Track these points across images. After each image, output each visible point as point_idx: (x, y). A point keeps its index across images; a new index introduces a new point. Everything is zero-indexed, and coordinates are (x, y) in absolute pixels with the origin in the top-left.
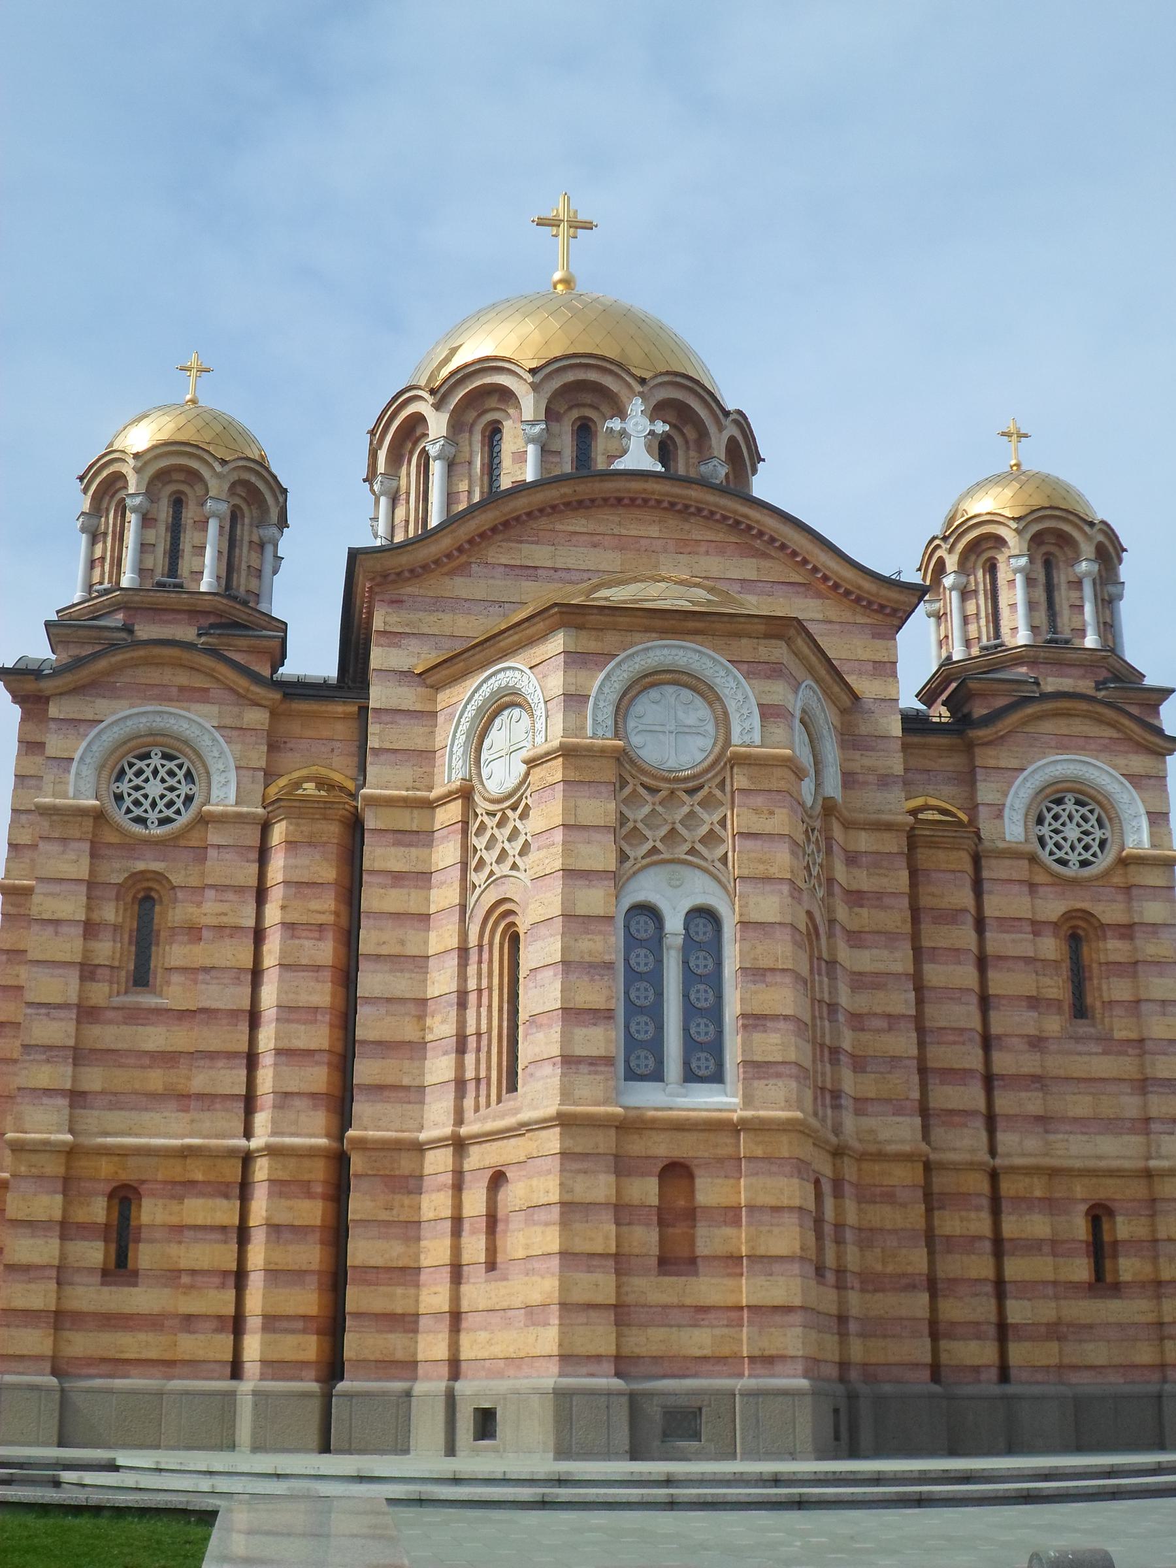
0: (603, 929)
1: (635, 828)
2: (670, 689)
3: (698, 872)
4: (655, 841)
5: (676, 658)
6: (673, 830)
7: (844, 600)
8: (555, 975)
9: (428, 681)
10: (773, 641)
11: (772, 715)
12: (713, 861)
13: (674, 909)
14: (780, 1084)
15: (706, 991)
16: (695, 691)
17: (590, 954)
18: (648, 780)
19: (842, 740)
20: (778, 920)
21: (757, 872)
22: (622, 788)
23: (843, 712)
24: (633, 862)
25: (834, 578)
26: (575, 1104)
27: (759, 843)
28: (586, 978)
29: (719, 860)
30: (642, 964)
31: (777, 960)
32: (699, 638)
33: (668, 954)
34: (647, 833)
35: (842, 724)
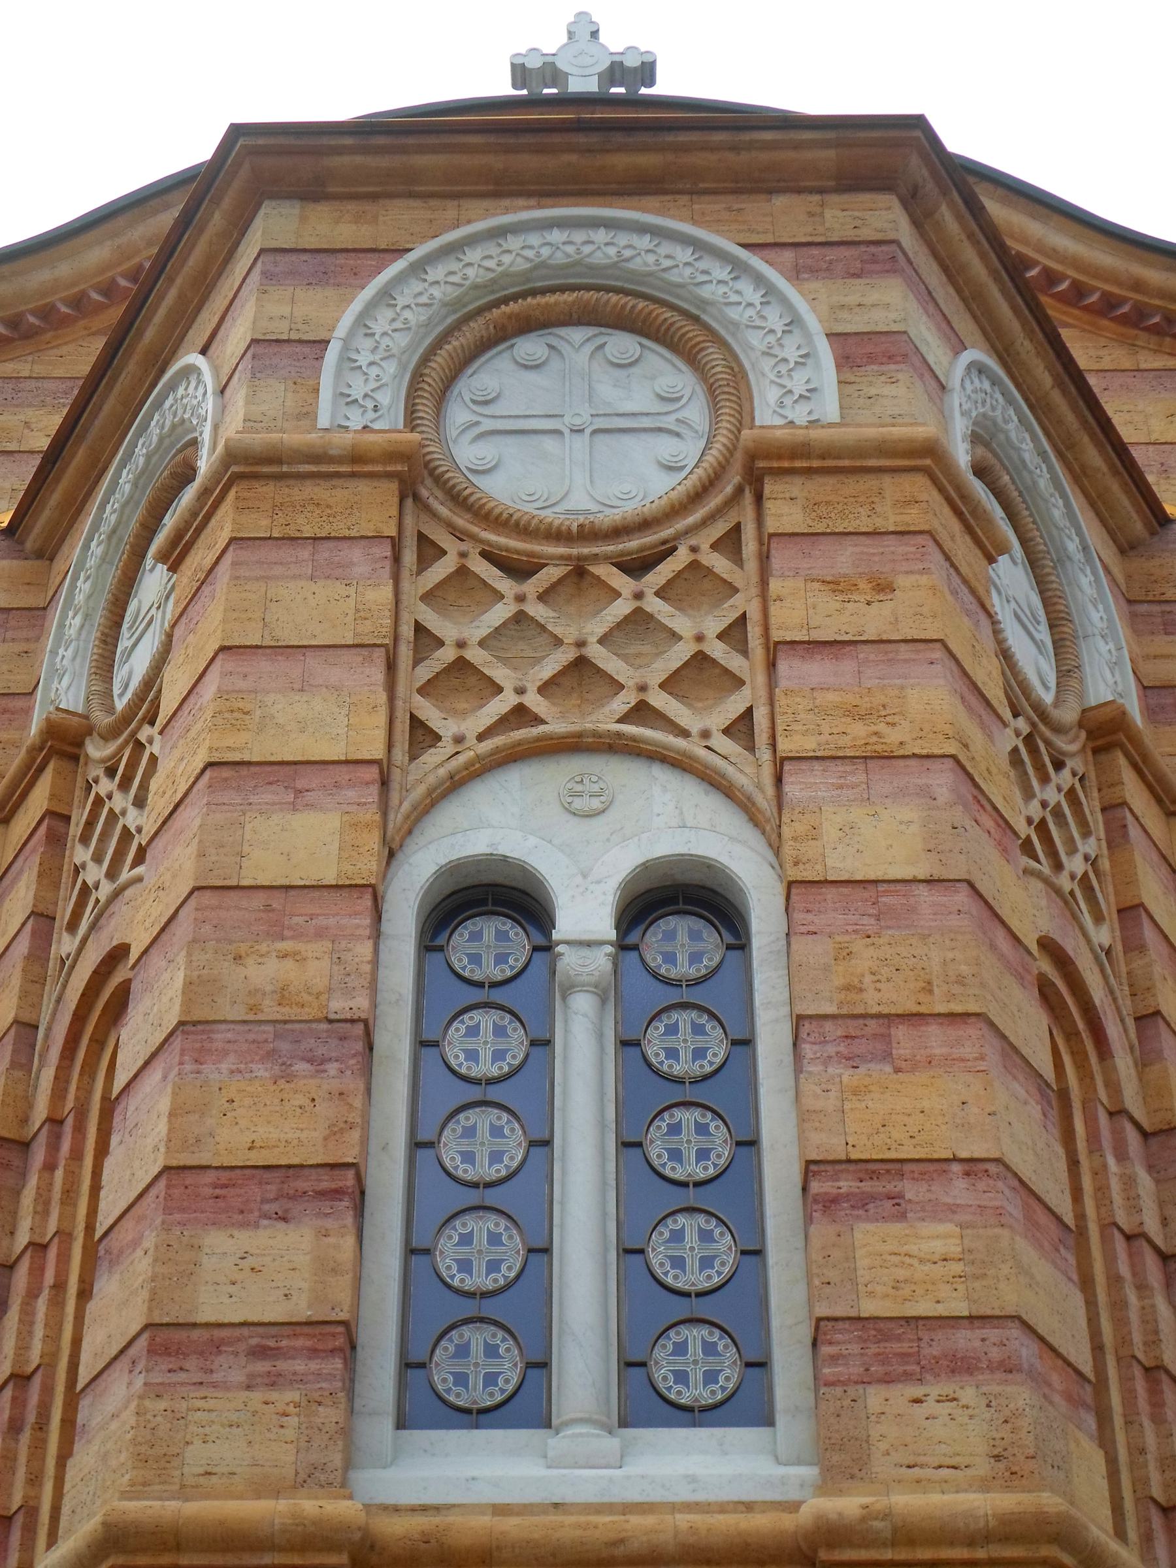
0: (332, 921)
1: (462, 665)
2: (577, 334)
3: (659, 772)
4: (520, 691)
5: (587, 249)
6: (581, 665)
7: (1105, 322)
8: (165, 1078)
9: (29, 545)
10: (865, 198)
11: (871, 358)
12: (705, 734)
13: (585, 876)
14: (968, 1395)
15: (702, 1129)
16: (647, 336)
17: (283, 995)
18: (502, 540)
19: (1133, 616)
20: (922, 871)
21: (844, 741)
22: (424, 563)
23: (1126, 547)
24: (450, 749)
25: (1071, 273)
26: (184, 1492)
27: (847, 666)
28: (262, 1071)
29: (726, 731)
30: (486, 1054)
31: (928, 989)
32: (653, 201)
33: (566, 1006)
34: (499, 673)
35: (1129, 577)
